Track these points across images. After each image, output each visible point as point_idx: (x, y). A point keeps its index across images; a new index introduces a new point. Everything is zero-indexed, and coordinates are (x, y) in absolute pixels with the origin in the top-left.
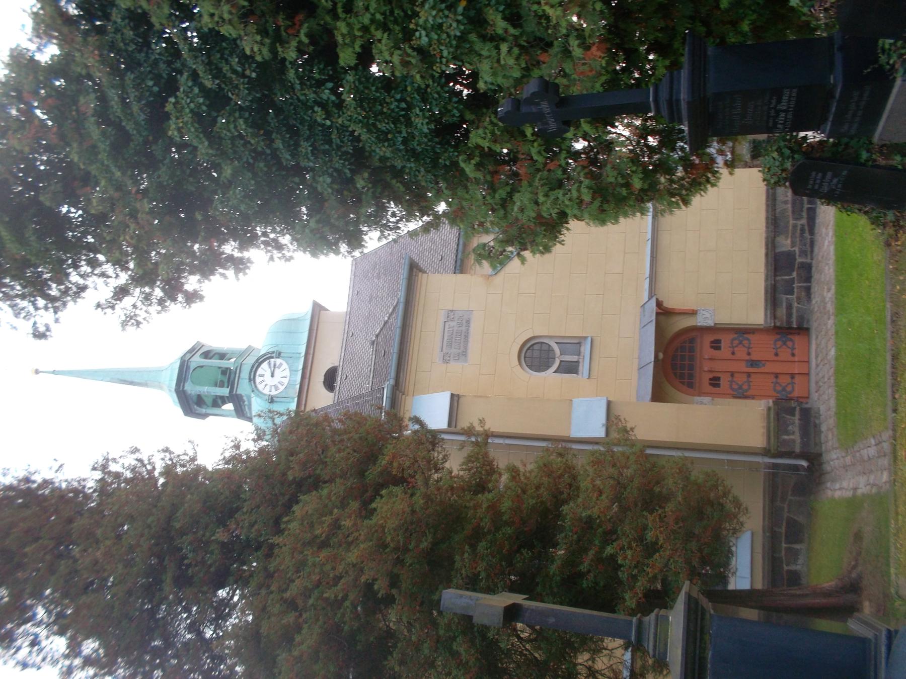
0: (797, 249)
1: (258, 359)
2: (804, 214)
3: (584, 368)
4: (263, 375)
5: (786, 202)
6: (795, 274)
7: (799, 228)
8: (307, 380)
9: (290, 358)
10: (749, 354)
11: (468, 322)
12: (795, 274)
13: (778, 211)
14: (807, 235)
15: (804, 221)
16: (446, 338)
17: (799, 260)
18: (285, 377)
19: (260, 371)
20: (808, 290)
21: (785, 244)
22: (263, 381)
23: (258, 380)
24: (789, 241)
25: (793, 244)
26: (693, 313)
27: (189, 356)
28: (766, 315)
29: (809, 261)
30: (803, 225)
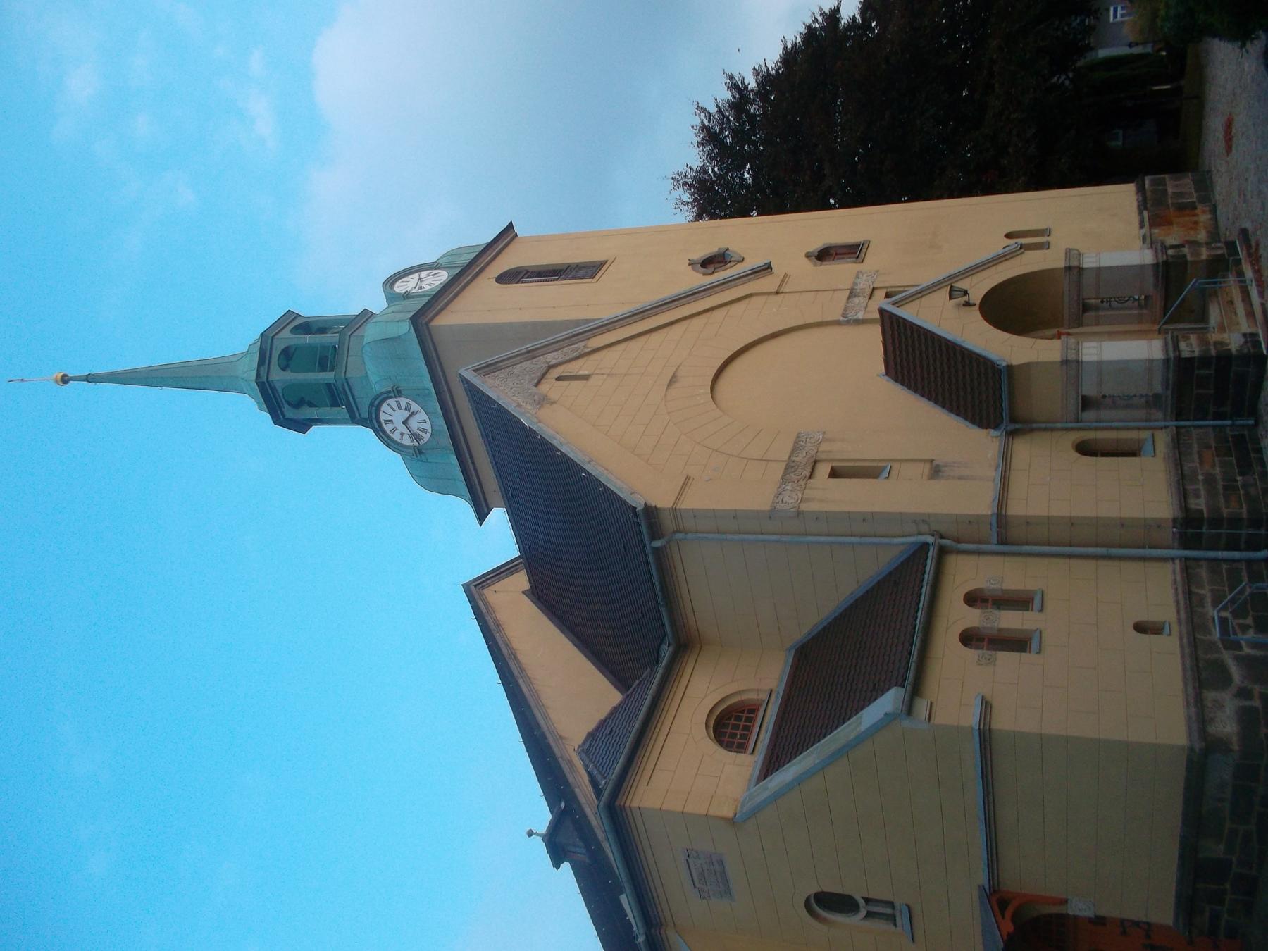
1: (372, 404)
3: (902, 920)
4: (391, 422)
9: (418, 396)
11: (721, 863)
12: (1228, 886)
19: (383, 417)
21: (1214, 849)
22: (396, 429)
23: (388, 428)
24: (1222, 847)
26: (1064, 902)
27: (263, 371)
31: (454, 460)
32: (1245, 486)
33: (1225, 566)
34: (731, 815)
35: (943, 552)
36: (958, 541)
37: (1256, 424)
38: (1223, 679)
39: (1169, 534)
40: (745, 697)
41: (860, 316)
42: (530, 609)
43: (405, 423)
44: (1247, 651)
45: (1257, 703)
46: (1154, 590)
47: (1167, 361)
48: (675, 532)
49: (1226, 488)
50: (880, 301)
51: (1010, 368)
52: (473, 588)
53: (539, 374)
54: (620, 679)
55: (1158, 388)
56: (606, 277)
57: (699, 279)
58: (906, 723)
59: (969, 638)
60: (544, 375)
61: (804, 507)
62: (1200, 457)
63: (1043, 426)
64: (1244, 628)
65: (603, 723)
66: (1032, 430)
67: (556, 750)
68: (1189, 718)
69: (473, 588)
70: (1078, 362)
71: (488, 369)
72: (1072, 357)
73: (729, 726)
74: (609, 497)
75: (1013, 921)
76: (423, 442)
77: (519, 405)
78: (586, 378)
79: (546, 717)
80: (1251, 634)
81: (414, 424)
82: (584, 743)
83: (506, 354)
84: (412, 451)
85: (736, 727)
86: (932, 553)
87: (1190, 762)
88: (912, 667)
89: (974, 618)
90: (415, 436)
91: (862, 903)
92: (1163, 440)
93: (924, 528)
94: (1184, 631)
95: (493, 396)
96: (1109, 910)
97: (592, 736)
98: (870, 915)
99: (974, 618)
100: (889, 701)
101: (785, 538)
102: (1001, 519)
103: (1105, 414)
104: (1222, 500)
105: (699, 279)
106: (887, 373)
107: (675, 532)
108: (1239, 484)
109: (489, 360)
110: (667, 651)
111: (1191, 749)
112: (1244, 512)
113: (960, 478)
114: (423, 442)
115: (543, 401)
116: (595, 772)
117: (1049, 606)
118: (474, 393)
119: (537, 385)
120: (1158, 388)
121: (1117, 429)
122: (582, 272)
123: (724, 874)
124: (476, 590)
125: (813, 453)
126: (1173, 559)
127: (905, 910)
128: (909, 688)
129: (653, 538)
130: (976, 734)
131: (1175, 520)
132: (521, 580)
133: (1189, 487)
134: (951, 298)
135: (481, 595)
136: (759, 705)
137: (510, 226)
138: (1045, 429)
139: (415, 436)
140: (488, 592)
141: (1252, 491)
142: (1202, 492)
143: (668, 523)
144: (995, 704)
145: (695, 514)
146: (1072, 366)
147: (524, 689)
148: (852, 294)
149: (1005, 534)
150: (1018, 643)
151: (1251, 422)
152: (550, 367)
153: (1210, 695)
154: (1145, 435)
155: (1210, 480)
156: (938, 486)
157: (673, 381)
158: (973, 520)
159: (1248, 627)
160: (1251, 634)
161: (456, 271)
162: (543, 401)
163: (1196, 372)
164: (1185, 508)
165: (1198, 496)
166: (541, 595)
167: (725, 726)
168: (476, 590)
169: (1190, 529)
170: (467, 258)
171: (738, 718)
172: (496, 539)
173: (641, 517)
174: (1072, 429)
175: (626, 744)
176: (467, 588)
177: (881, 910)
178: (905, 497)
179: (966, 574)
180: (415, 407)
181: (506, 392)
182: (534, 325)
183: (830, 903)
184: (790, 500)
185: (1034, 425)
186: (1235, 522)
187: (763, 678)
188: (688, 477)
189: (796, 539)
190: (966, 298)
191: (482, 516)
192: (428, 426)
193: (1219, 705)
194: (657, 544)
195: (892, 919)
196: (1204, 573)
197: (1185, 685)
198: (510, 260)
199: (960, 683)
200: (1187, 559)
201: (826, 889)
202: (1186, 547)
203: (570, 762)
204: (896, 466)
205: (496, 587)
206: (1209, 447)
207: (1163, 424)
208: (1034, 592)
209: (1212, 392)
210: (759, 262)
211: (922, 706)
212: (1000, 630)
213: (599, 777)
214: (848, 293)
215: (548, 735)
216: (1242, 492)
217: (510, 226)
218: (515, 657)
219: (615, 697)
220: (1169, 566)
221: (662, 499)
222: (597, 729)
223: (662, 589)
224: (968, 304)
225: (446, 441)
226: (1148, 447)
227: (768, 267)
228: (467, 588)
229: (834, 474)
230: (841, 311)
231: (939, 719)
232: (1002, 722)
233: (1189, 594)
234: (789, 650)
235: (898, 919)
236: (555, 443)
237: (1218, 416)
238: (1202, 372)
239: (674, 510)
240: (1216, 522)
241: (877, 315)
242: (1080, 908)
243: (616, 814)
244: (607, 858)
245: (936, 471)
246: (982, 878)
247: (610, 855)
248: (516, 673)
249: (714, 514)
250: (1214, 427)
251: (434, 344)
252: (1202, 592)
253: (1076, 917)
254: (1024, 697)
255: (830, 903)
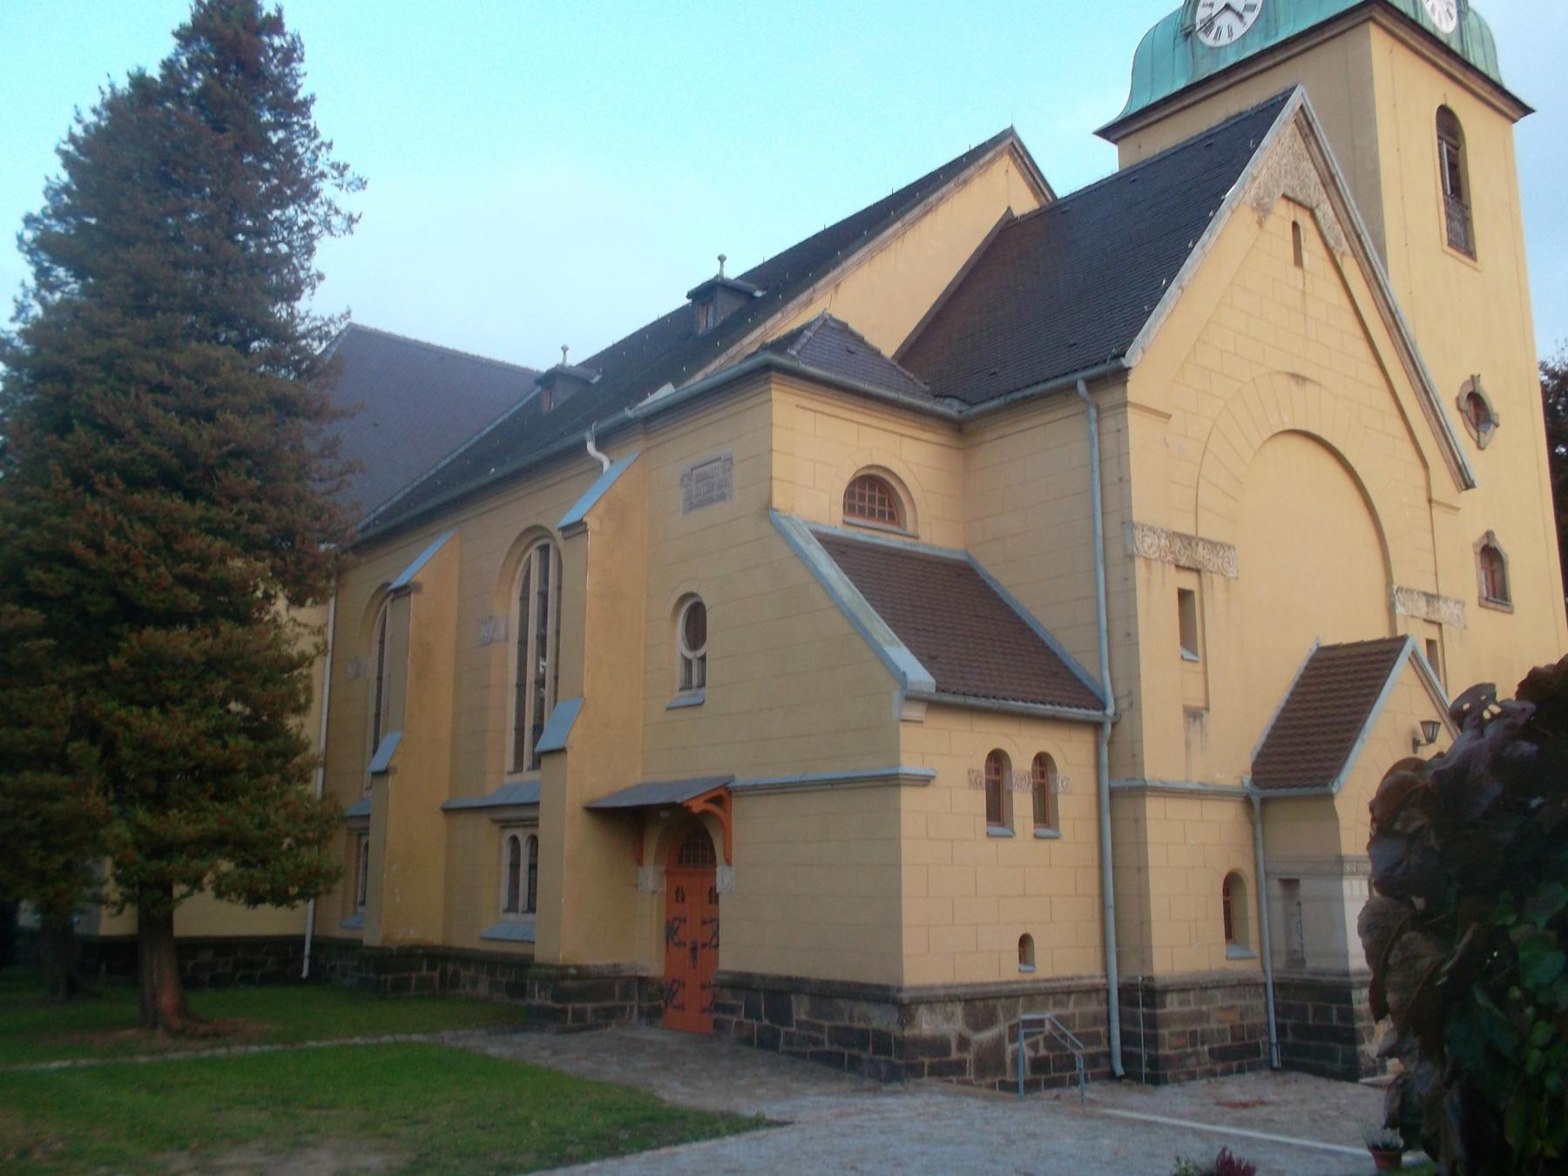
0: (794, 1029)
2: (835, 1048)
3: (687, 697)
5: (851, 1017)
6: (766, 1022)
7: (820, 1036)
8: (1226, 83)
10: (704, 945)
11: (722, 497)
13: (841, 1002)
14: (811, 1049)
15: (827, 1047)
16: (706, 468)
17: (783, 1030)
18: (1230, 34)
20: (748, 1042)
21: (801, 1010)
24: (803, 1017)
25: (800, 1024)
26: (728, 862)
28: (725, 973)
29: (782, 1047)
30: (822, 1042)
31: (1180, 84)
32: (1197, 1054)
33: (1102, 1029)
34: (775, 505)
35: (1097, 726)
36: (1110, 743)
37: (1273, 1069)
38: (977, 1028)
39: (1136, 974)
40: (907, 507)
41: (1400, 610)
42: (989, 221)
43: (1227, 7)
44: (1010, 1048)
45: (955, 1055)
46: (1069, 954)
47: (1347, 974)
48: (1097, 407)
49: (1193, 1034)
50: (1417, 636)
51: (1330, 797)
52: (1009, 140)
53: (1300, 197)
54: (912, 351)
55: (1311, 964)
56: (1454, 263)
57: (1448, 394)
58: (897, 695)
59: (997, 760)
60: (1300, 204)
61: (1139, 563)
62: (1232, 1008)
63: (1259, 836)
64: (1034, 1046)
65: (860, 340)
66: (1253, 824)
67: (823, 282)
68: (932, 988)
69: (1009, 140)
70: (1340, 875)
71: (1305, 127)
72: (1348, 867)
73: (873, 492)
74: (1136, 322)
75: (706, 813)
76: (1201, 36)
77: (1254, 179)
78: (1298, 261)
79: (859, 263)
80: (1028, 1053)
81: (1227, 20)
82: (835, 320)
83: (1327, 146)
84: (1188, 23)
85: (872, 499)
86: (1095, 714)
87: (887, 988)
88: (959, 700)
89: (1021, 763)
90: (1209, 24)
91: (700, 653)
92: (1247, 967)
93: (1124, 704)
94: (1027, 986)
95: (1265, 142)
96: (725, 908)
97: (844, 329)
98: (688, 663)
99: (1021, 763)
100: (919, 676)
101: (1099, 542)
102: (1140, 791)
103: (1278, 906)
104: (1178, 1028)
105: (1448, 394)
106: (1321, 649)
107: (1097, 407)
108: (1199, 1048)
109: (1318, 126)
110: (951, 408)
111: (900, 989)
112: (1165, 1051)
113: (1187, 744)
114: (1201, 36)
115: (1262, 210)
116: (804, 340)
117: (1044, 844)
118: (1270, 110)
119: (1285, 197)
120: (1311, 964)
121: (1260, 919)
122: (1456, 225)
123: (709, 501)
124: (1007, 145)
125: (1210, 567)
126: (1107, 976)
127: (698, 700)
128: (936, 697)
129: (1089, 382)
130: (893, 771)
131: (1151, 979)
132: (1024, 203)
133: (1192, 995)
134: (1424, 724)
135: (1001, 154)
136: (899, 525)
137: (1527, 110)
138: (1255, 838)
139: (1209, 24)
140: (1005, 162)
141: (1192, 1061)
142: (1186, 1009)
143: (1108, 398)
144: (928, 790)
145: (1122, 431)
146: (1336, 867)
147: (890, 231)
148: (1431, 598)
149: (1122, 796)
150: (997, 811)
151: (1276, 1064)
152: (1312, 212)
153: (959, 1009)
154: (1254, 950)
155: (1201, 1017)
156: (1178, 718)
157: (1298, 378)
158: (1136, 758)
159: (1037, 1052)
160: (1028, 1053)
161: (1455, 46)
162: (1262, 210)
163: (1334, 1007)
164: (1165, 991)
165: (1181, 1003)
166: (1008, 231)
167: (872, 487)
168: (1007, 145)
169: (1142, 996)
170: (1476, 57)
171: (882, 502)
172: (1078, 161)
173: (1113, 365)
174: (1256, 867)
175: (838, 371)
176: (1009, 133)
177: (694, 675)
178: (1160, 679)
179: (1073, 755)
180: (1250, 18)
181: (1276, 153)
182: (1375, 173)
183: (696, 620)
184: (1147, 544)
185: (1259, 826)
186: (1153, 1041)
187: (931, 527)
188: (1168, 416)
189: (1100, 557)
190: (1424, 741)
191: (1106, 133)
192: (1225, 40)
193: (949, 1018)
194: (1081, 387)
195: (687, 685)
196: (1093, 1007)
197: (967, 986)
198: (1474, 117)
199: (946, 753)
200: (1108, 991)
201: (709, 615)
202: (1120, 990)
203: (810, 302)
204: (1200, 668)
205: (1014, 171)
206: (1242, 1017)
207: (1268, 967)
208: (1056, 827)
209: (1310, 1022)
210: (1475, 473)
211: (916, 712)
212: (1010, 793)
213: (798, 347)
214: (1433, 591)
215: (839, 269)
216: (1189, 1050)
217: (1527, 110)
218: (926, 213)
219: (889, 348)
220: (1098, 972)
221: (1136, 389)
222: (852, 334)
223: (1025, 399)
224: (1416, 744)
225: (1205, 71)
226: (1237, 952)
227: (1468, 485)
228: (1009, 133)
229: (1184, 595)
230: (1405, 586)
231: (905, 731)
232: (909, 799)
233: (1068, 992)
234: (966, 553)
235: (686, 693)
236: (1205, 237)
237: (1281, 1030)
238: (1335, 1012)
239: (1125, 404)
240: (1152, 1022)
241: (1400, 633)
242: (724, 878)
243: (757, 375)
244: (710, 362)
245: (1194, 715)
246: (741, 779)
247: (712, 367)
248: (908, 217)
249: (1122, 456)
250: (1268, 1024)
251: (1343, 32)
252: (1071, 1003)
253: (715, 874)
254: (939, 821)
255: (696, 620)
